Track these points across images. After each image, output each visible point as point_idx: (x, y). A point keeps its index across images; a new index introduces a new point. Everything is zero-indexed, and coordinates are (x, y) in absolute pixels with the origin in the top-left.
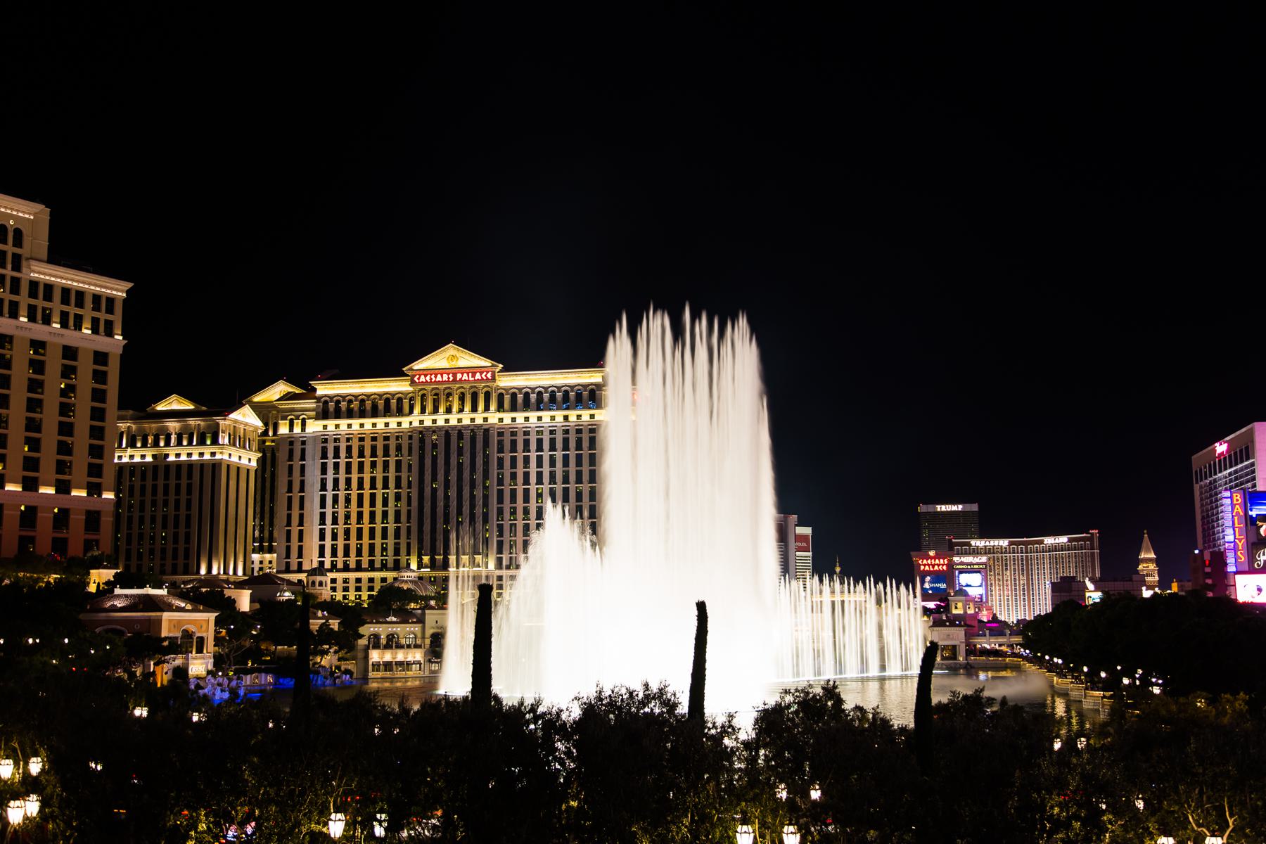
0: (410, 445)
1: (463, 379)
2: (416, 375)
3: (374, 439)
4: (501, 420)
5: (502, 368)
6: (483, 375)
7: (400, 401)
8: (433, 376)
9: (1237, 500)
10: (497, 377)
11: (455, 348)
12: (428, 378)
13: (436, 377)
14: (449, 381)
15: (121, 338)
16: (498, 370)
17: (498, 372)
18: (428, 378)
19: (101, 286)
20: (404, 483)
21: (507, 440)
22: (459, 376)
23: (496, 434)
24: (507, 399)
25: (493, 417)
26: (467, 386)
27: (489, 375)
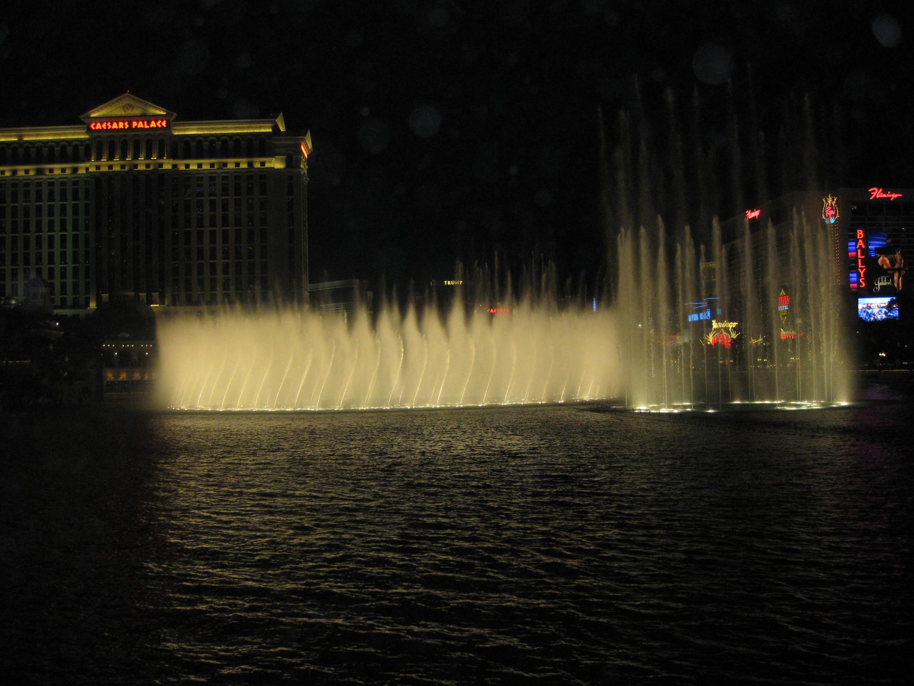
1: (139, 127)
5: (177, 117)
6: (158, 124)
8: (109, 124)
9: (860, 236)
12: (104, 126)
13: (112, 125)
16: (172, 119)
17: (173, 121)
20: (81, 225)
22: (134, 124)
25: (167, 165)
27: (164, 124)
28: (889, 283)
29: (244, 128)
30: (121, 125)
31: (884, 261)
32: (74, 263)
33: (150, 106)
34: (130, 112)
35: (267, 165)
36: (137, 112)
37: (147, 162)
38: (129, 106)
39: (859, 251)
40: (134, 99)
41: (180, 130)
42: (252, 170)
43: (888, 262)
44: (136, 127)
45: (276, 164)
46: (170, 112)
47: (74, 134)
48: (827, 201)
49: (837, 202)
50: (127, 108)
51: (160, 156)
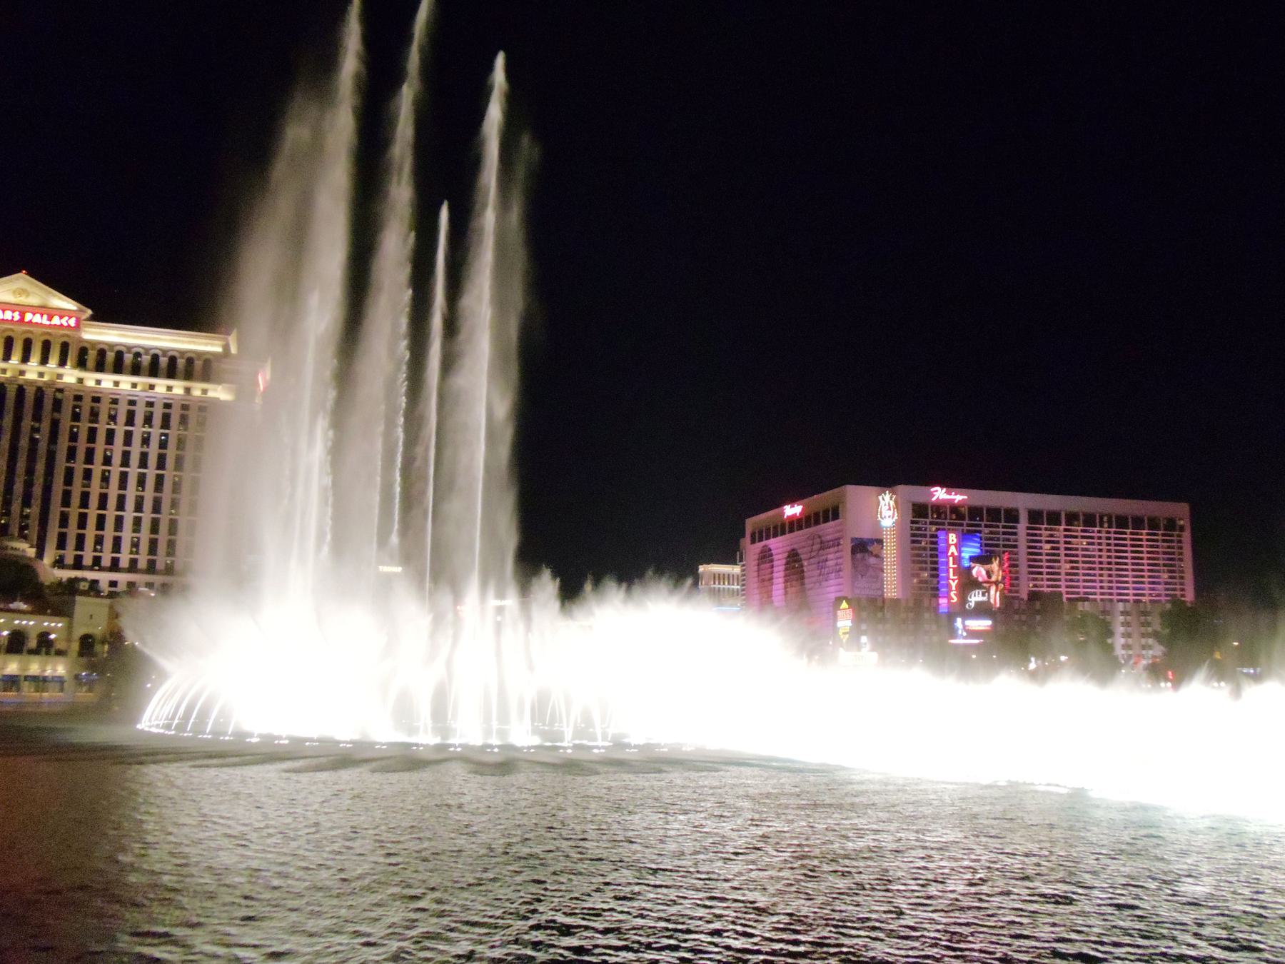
6: (64, 321)
10: (81, 326)
14: (12, 320)
17: (85, 320)
21: (87, 405)
22: (28, 317)
23: (72, 398)
25: (70, 376)
26: (39, 330)
27: (72, 322)
28: (985, 599)
31: (979, 571)
33: (54, 296)
35: (211, 394)
36: (34, 300)
37: (42, 369)
38: (23, 292)
39: (951, 559)
41: (91, 333)
42: (188, 397)
43: (984, 573)
44: (30, 321)
48: (883, 499)
49: (896, 502)
51: (62, 363)
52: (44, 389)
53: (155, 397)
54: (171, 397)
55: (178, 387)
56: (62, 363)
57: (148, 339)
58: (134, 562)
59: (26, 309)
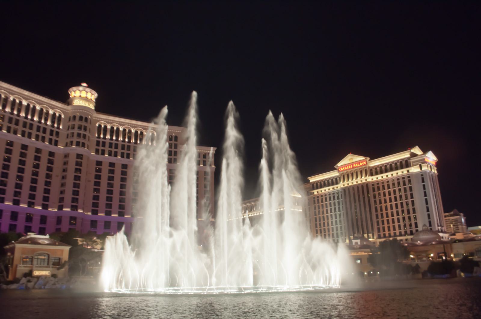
0: (341, 194)
2: (339, 169)
3: (329, 194)
4: (372, 179)
7: (336, 179)
8: (345, 167)
11: (351, 155)
12: (344, 169)
13: (346, 167)
15: (214, 166)
18: (344, 169)
19: (206, 150)
22: (354, 165)
24: (374, 170)
25: (369, 179)
27: (365, 163)
29: (397, 157)
30: (350, 167)
32: (340, 224)
34: (352, 161)
38: (352, 159)
40: (352, 156)
44: (355, 167)
45: (414, 170)
46: (366, 158)
47: (335, 174)
50: (351, 160)
52: (359, 186)
53: (394, 178)
54: (393, 177)
55: (400, 172)
56: (366, 176)
57: (387, 160)
58: (400, 233)
59: (353, 163)
